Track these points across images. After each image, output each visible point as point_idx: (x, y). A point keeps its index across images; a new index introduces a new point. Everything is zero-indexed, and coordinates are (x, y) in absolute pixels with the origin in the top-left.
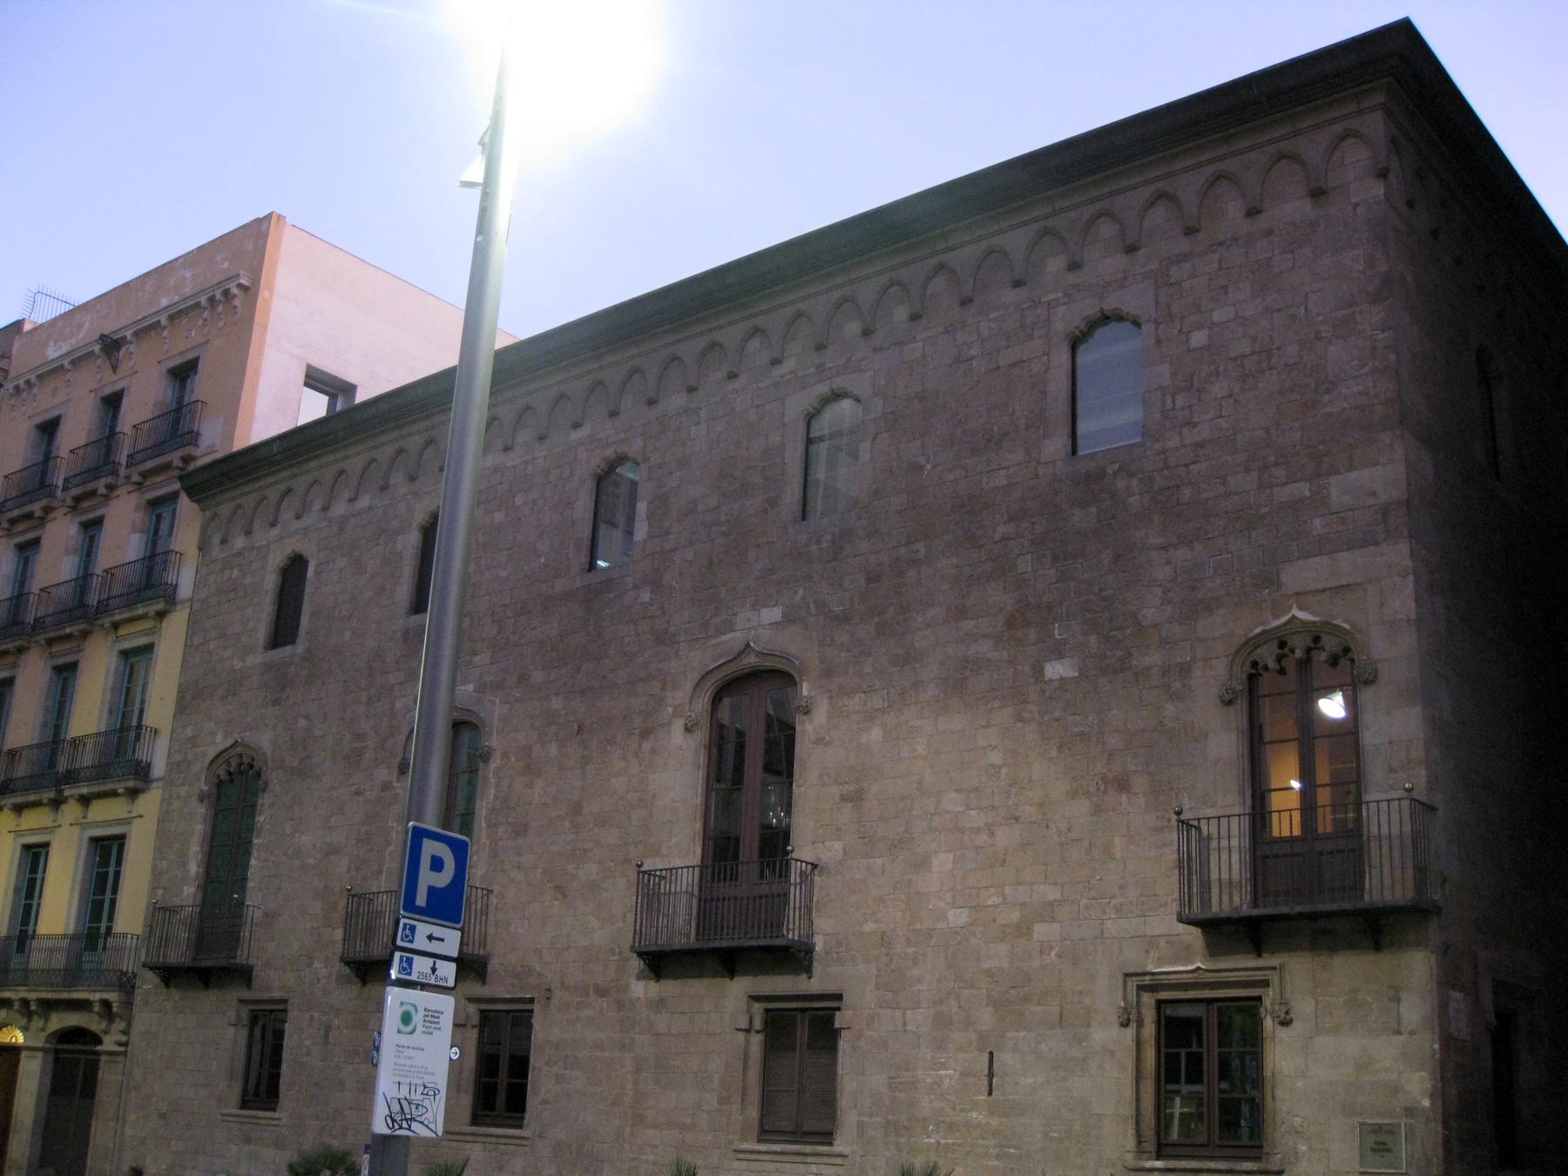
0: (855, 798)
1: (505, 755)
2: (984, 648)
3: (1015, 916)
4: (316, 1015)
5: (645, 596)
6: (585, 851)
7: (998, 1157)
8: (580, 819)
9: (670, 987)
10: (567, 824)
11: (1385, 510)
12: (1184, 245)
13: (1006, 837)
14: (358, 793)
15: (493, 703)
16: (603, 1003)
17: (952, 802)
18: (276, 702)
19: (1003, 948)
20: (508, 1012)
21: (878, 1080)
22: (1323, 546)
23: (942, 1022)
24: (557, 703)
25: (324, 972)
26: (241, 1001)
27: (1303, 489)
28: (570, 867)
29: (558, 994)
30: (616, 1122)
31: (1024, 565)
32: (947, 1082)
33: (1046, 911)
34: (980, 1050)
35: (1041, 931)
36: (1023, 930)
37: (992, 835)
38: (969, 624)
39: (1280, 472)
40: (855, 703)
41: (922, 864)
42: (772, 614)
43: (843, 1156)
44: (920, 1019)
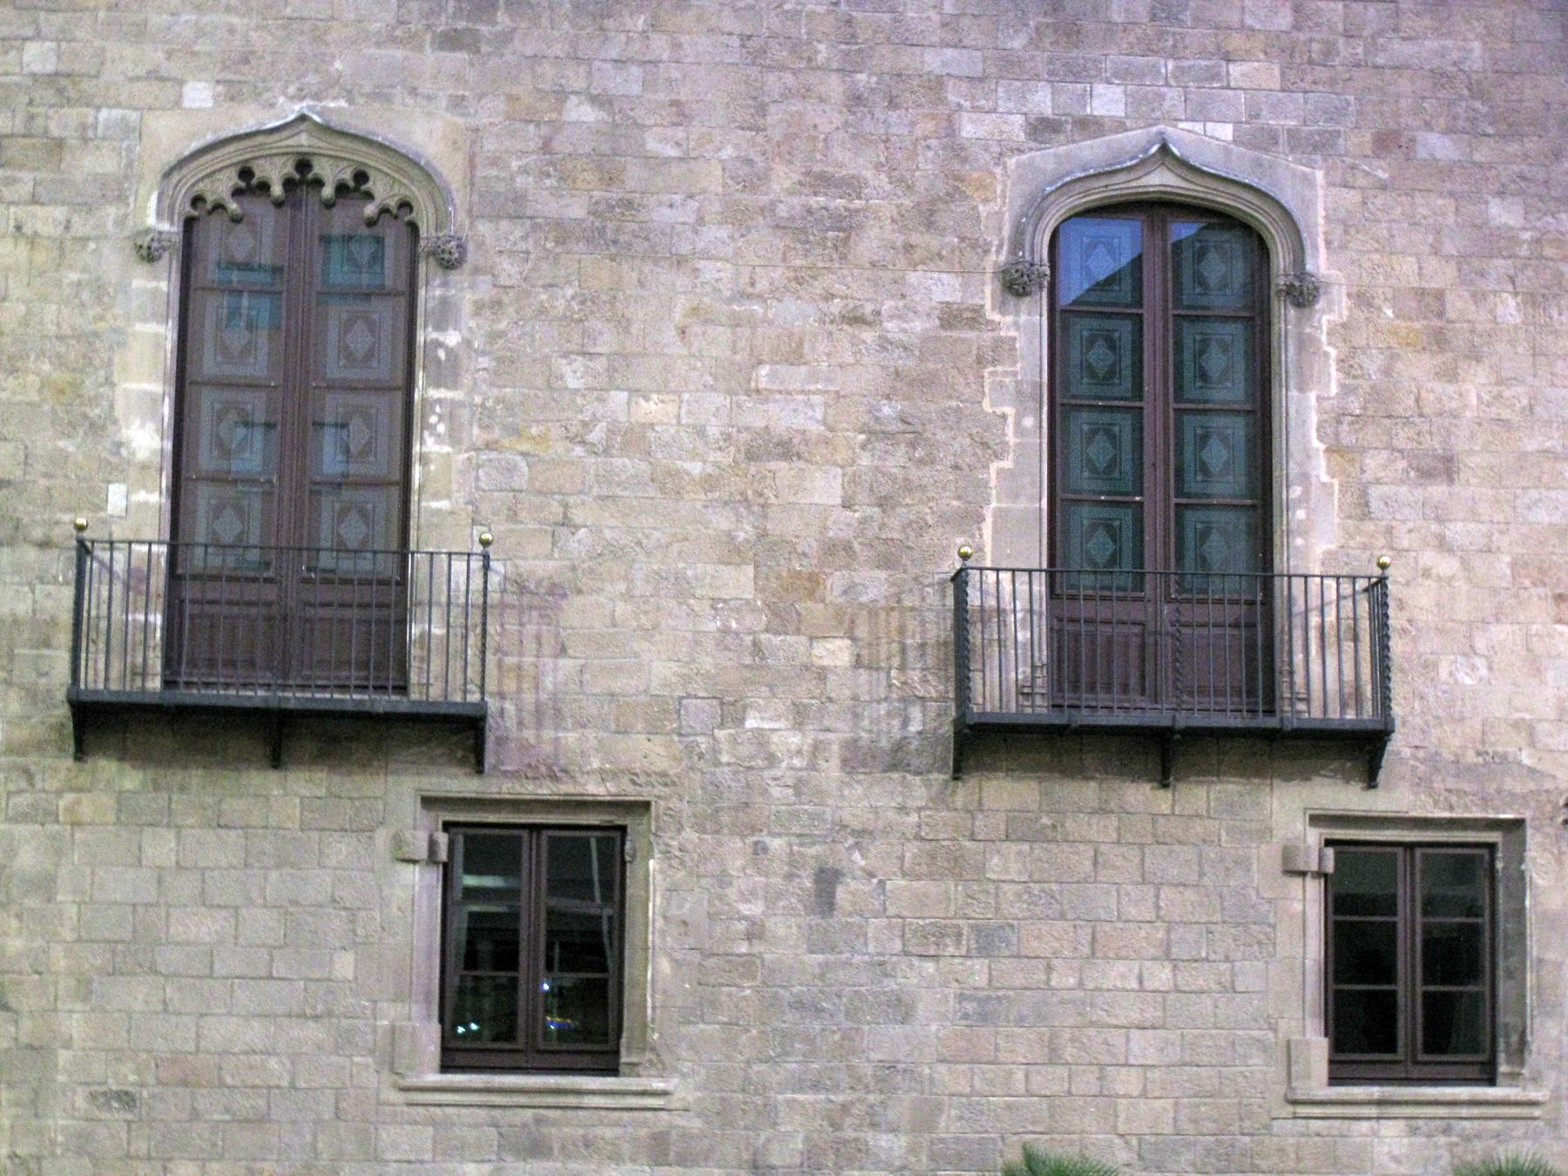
1: (1362, 299)
4: (776, 844)
14: (855, 319)
15: (1308, 181)
18: (450, 41)
20: (1410, 846)
24: (1503, 214)
25: (788, 740)
26: (429, 802)
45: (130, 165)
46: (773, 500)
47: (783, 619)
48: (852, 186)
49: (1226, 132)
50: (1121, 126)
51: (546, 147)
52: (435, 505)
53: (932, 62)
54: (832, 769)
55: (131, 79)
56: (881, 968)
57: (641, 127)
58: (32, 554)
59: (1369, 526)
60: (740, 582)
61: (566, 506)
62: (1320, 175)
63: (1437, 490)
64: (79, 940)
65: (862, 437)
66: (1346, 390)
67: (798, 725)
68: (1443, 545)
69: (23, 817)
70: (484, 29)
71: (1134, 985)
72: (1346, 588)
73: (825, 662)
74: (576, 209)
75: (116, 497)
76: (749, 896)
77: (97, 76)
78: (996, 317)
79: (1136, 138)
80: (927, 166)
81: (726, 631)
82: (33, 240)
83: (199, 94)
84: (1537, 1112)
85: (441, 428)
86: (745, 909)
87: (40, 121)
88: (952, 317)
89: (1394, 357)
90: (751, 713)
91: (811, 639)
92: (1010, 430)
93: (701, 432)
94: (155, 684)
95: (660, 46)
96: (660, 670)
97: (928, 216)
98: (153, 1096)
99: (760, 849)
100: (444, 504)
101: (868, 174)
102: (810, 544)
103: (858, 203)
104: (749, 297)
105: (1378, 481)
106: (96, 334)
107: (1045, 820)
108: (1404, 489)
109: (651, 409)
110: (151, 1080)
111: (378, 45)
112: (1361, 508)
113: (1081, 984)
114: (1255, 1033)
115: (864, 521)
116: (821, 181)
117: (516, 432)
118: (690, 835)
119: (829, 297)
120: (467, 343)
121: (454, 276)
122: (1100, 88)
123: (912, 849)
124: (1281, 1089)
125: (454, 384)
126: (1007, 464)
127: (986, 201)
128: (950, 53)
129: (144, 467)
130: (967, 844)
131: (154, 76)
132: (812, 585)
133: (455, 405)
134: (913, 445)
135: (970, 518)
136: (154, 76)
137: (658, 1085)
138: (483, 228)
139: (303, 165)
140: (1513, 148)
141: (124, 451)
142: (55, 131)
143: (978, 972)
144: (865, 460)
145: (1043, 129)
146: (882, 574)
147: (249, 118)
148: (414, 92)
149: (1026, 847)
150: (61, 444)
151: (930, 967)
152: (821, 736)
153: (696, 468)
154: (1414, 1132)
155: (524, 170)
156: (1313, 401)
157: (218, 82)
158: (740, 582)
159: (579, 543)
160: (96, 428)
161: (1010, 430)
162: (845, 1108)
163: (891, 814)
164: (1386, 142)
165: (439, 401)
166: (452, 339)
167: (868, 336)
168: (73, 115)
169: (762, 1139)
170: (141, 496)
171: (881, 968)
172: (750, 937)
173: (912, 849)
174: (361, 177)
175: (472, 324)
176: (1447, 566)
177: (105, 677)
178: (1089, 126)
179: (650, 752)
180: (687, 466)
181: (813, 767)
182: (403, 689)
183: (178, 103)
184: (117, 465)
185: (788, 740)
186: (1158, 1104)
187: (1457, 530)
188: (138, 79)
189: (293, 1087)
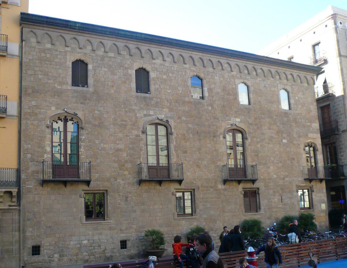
0: (257, 156)
1: (177, 134)
2: (274, 135)
3: (283, 177)
5: (210, 108)
6: (203, 159)
7: (284, 212)
8: (201, 152)
9: (226, 186)
10: (198, 153)
11: (317, 130)
12: (294, 83)
13: (280, 165)
14: (127, 136)
16: (212, 190)
17: (272, 159)
18: (82, 103)
19: (281, 181)
21: (266, 201)
22: (312, 132)
23: (274, 192)
25: (122, 182)
27: (309, 124)
28: (200, 162)
29: (200, 188)
30: (219, 213)
31: (278, 124)
32: (276, 201)
33: (287, 176)
34: (280, 196)
35: (286, 179)
36: (284, 179)
37: (278, 164)
38: (271, 131)
39: (307, 121)
40: (255, 139)
41: (269, 168)
42: (238, 120)
43: (262, 214)
44: (271, 192)
45: (45, 116)
46: (119, 156)
47: (121, 169)
48: (126, 121)
49: (163, 116)
50: (153, 115)
51: (93, 116)
52: (82, 157)
53: (134, 107)
54: (127, 186)
55: (45, 106)
56: (133, 207)
57: (103, 114)
58: (36, 163)
59: (179, 158)
60: (116, 165)
61: (97, 156)
62: (173, 121)
63: (185, 155)
64: (43, 209)
65: (128, 149)
66: (176, 144)
67: (123, 181)
68: (186, 160)
69: (36, 194)
70: (86, 102)
71: (158, 208)
72: (177, 165)
73: (125, 174)
74: (97, 123)
75: (45, 155)
76: (118, 200)
77: (41, 106)
78: (141, 136)
79: (154, 117)
80: (134, 119)
81: (115, 170)
82: (34, 125)
83: (53, 108)
84: (197, 219)
85: (83, 148)
86: (118, 201)
87: (34, 111)
88: (137, 136)
89: (180, 141)
90: (118, 180)
91: (124, 171)
92: (143, 148)
93: (111, 148)
94: (51, 178)
95: (105, 104)
96: (108, 175)
97: (134, 125)
98: (53, 226)
99: (119, 195)
100: (84, 157)
101: (128, 120)
102: (123, 161)
103: (127, 123)
104: (116, 133)
105: (179, 154)
106: (42, 136)
107: (149, 190)
108: (182, 154)
109: (105, 146)
110: (53, 225)
111: (74, 103)
112: (178, 156)
113: (153, 208)
114: (170, 212)
115: (129, 158)
116: (123, 121)
117: (91, 148)
118: (112, 193)
119: (124, 133)
120: (85, 138)
121: (83, 130)
122: (151, 111)
123: (135, 194)
124: (173, 218)
125: (84, 143)
126: (143, 152)
127: (140, 123)
128: (136, 107)
129: (49, 152)
130: (141, 193)
131: (48, 106)
132: (124, 165)
133: (84, 145)
134: (133, 150)
135: (140, 158)
136: (48, 106)
137: (110, 221)
138: (87, 125)
139: (65, 117)
140: (191, 119)
141: (46, 151)
142: (36, 112)
143: (143, 207)
144: (129, 151)
145: (145, 115)
146: (131, 164)
147: (59, 111)
148: (78, 109)
149: (147, 193)
150: (39, 149)
151: (138, 207)
152: (126, 182)
153: (111, 152)
154: (186, 222)
155: (91, 118)
156: (173, 145)
157: (55, 107)
158: (116, 165)
159: (98, 161)
160: (43, 148)
161: (143, 148)
162: (130, 223)
163: (133, 190)
164: (179, 118)
165: (82, 145)
166: (83, 137)
167: (128, 138)
168: (39, 110)
169: (121, 227)
170: (49, 156)
171: (133, 207)
172: (119, 204)
173: (135, 194)
174: (72, 119)
175: (86, 136)
176: (186, 162)
177: (46, 178)
178: (150, 115)
179: (107, 184)
180: (110, 152)
181: (124, 185)
182: (79, 178)
183: (51, 109)
184: (46, 152)
185: (122, 182)
186: (161, 220)
187: (187, 159)
188: (46, 106)
189: (69, 224)
